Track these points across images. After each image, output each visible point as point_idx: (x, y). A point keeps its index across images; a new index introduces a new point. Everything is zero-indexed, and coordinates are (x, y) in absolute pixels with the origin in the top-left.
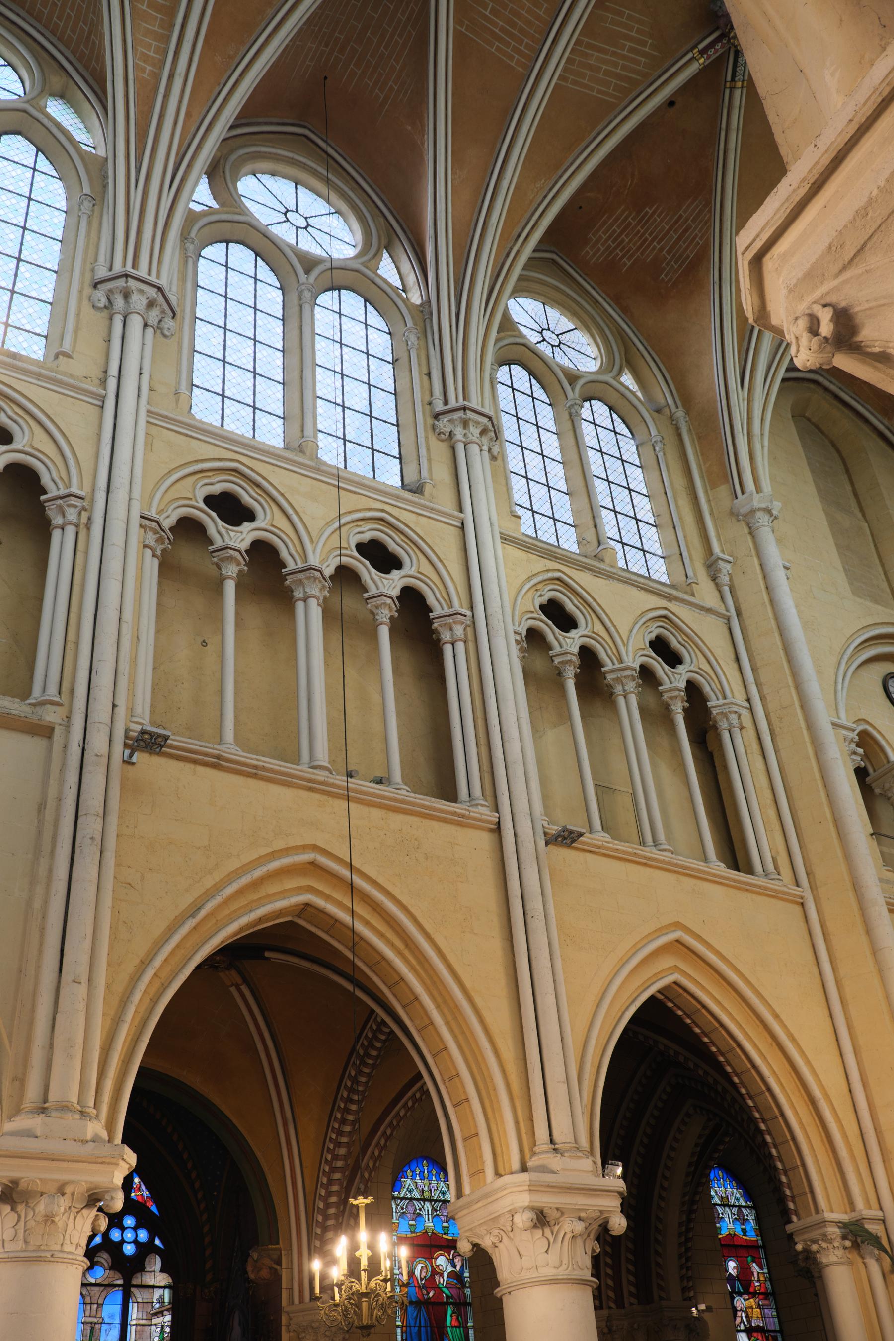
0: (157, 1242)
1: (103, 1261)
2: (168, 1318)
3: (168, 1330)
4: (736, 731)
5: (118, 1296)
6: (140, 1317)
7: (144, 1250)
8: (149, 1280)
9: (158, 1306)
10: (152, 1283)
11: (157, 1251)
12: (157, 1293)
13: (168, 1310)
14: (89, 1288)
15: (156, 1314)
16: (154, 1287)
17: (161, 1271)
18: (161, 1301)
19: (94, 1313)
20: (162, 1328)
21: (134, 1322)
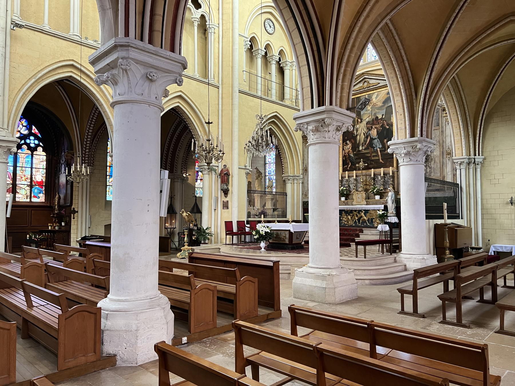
0: (41, 144)
2: (45, 163)
4: (213, 34)
5: (30, 157)
7: (38, 146)
11: (41, 146)
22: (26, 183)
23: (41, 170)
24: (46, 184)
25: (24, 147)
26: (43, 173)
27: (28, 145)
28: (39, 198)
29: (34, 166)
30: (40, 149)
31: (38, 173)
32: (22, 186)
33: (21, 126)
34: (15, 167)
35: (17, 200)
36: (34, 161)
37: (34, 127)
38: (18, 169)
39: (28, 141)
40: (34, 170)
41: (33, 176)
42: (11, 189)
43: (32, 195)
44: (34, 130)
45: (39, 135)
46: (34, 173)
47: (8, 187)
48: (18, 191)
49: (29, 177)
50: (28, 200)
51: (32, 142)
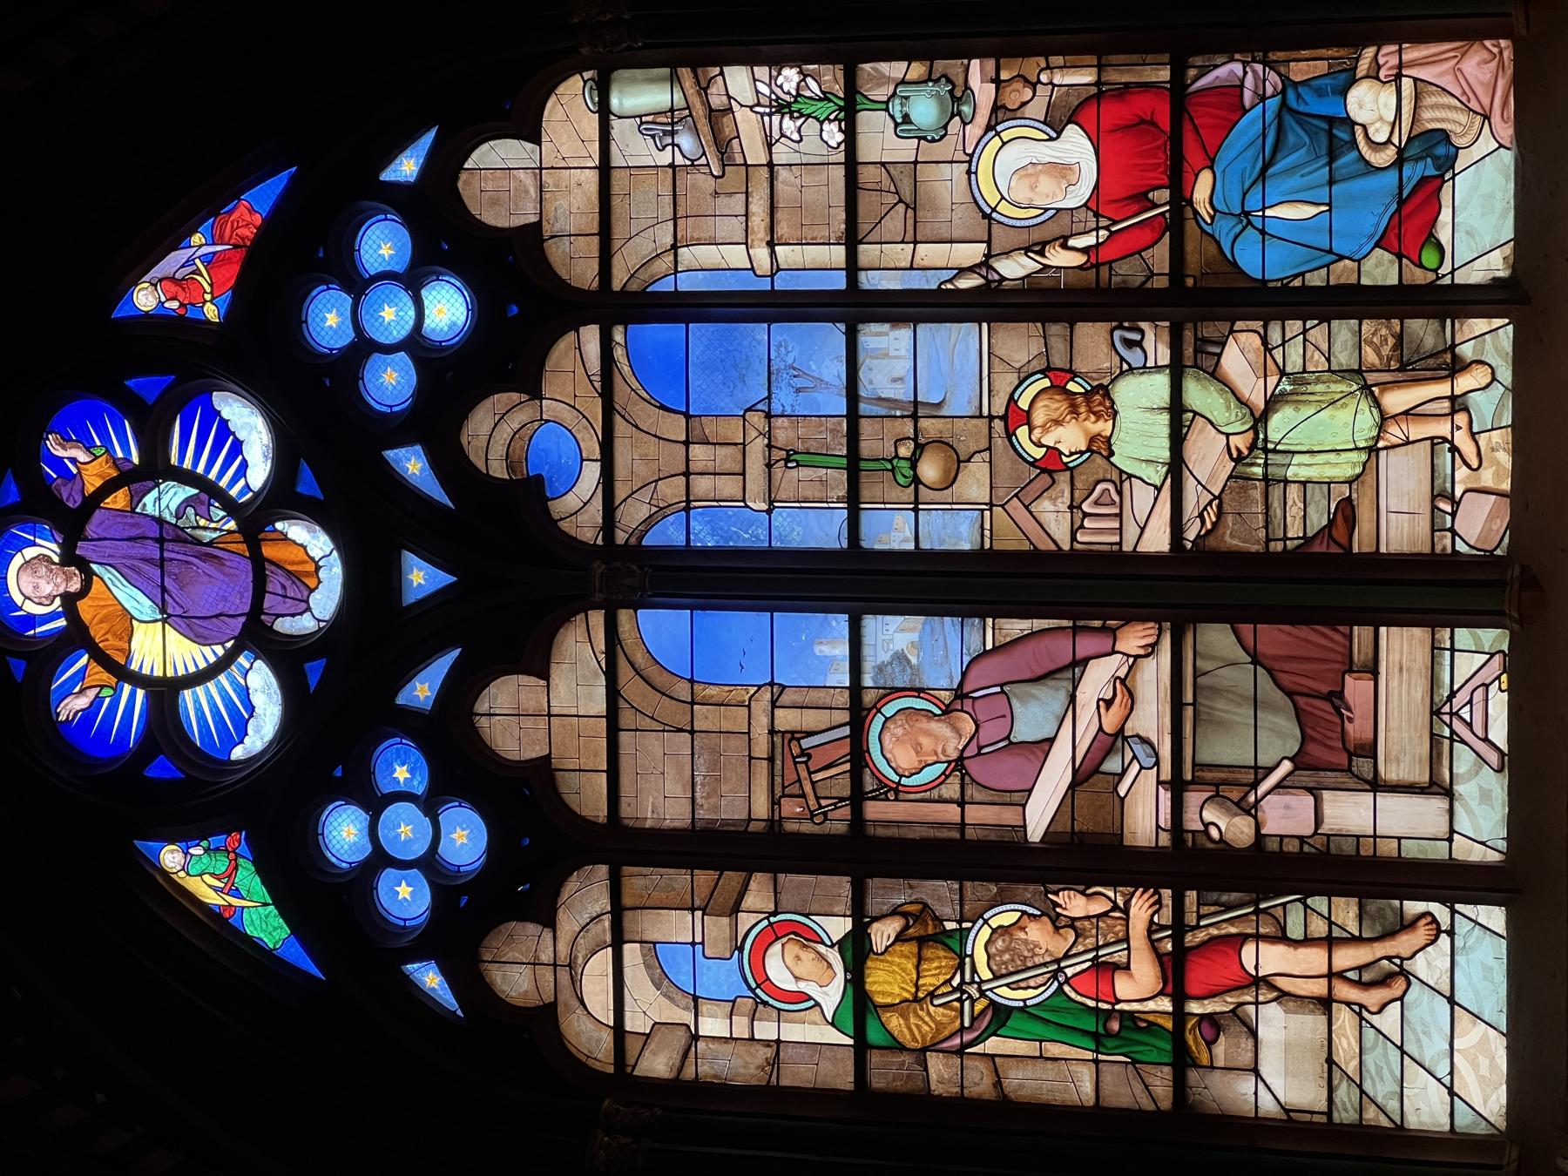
0: (407, 167)
1: (505, 432)
2: (739, 82)
3: (789, 78)
6: (737, 225)
7: (448, 236)
8: (573, 202)
9: (686, 141)
10: (591, 179)
11: (445, 166)
12: (632, 148)
13: (704, 90)
14: (621, 492)
15: (723, 146)
16: (605, 169)
17: (535, 137)
18: (663, 125)
19: (726, 457)
20: (782, 108)
21: (761, 254)
22: (1142, 397)
23: (879, 139)
24: (1141, 45)
25: (492, 432)
26: (925, 109)
27: (453, 381)
28: (1431, 154)
29: (815, 261)
30: (499, 177)
31: (946, 183)
32: (1208, 460)
33: (167, 499)
34: (858, 582)
35: (1480, 525)
36: (723, 257)
37: (145, 299)
38: (891, 530)
39: (391, 382)
40: (890, 266)
41: (1014, 268)
42: (1273, 637)
43: (1381, 270)
44: (184, 280)
45: (250, 212)
46: (947, 259)
47: (1242, 677)
48: (1300, 519)
49: (1020, 344)
50: (1489, 340)
51: (391, 316)
